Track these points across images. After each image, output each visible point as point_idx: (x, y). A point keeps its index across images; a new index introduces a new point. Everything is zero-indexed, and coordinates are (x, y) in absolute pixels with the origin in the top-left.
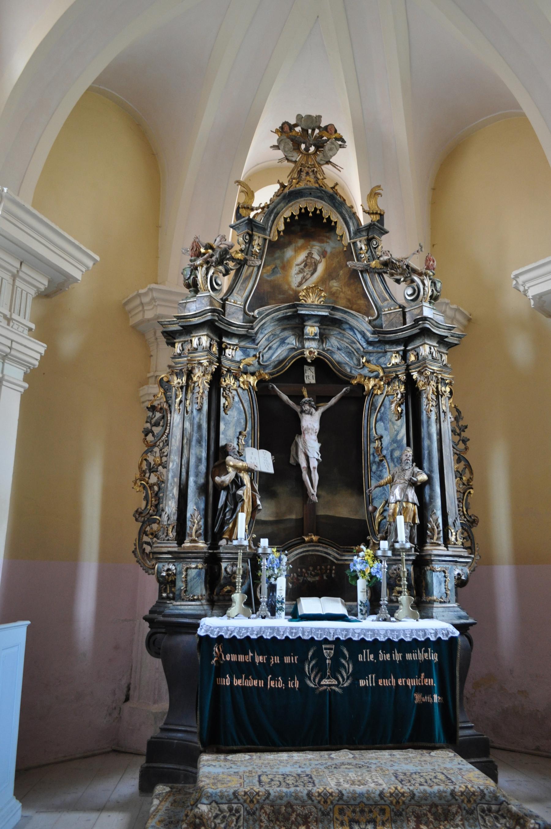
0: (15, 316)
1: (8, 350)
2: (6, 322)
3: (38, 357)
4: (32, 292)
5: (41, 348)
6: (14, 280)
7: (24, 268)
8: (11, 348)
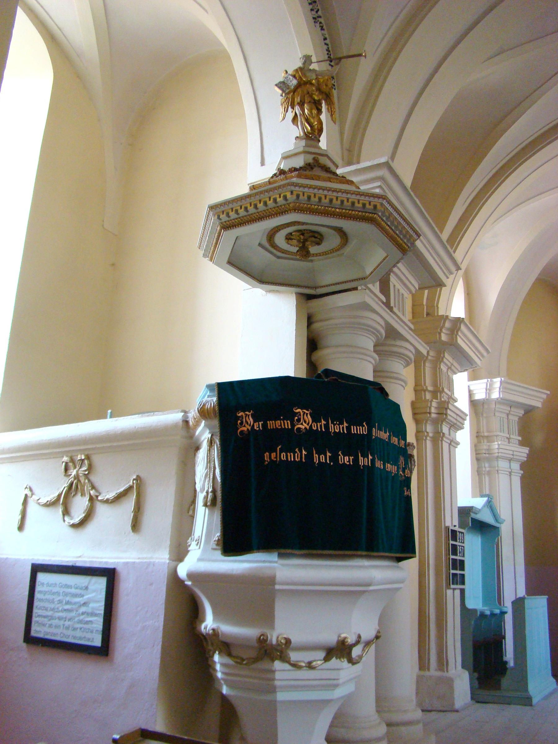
0: (512, 436)
1: (512, 457)
2: (507, 440)
3: (526, 455)
4: (516, 419)
5: (526, 450)
6: (508, 416)
7: (512, 409)
8: (513, 455)
